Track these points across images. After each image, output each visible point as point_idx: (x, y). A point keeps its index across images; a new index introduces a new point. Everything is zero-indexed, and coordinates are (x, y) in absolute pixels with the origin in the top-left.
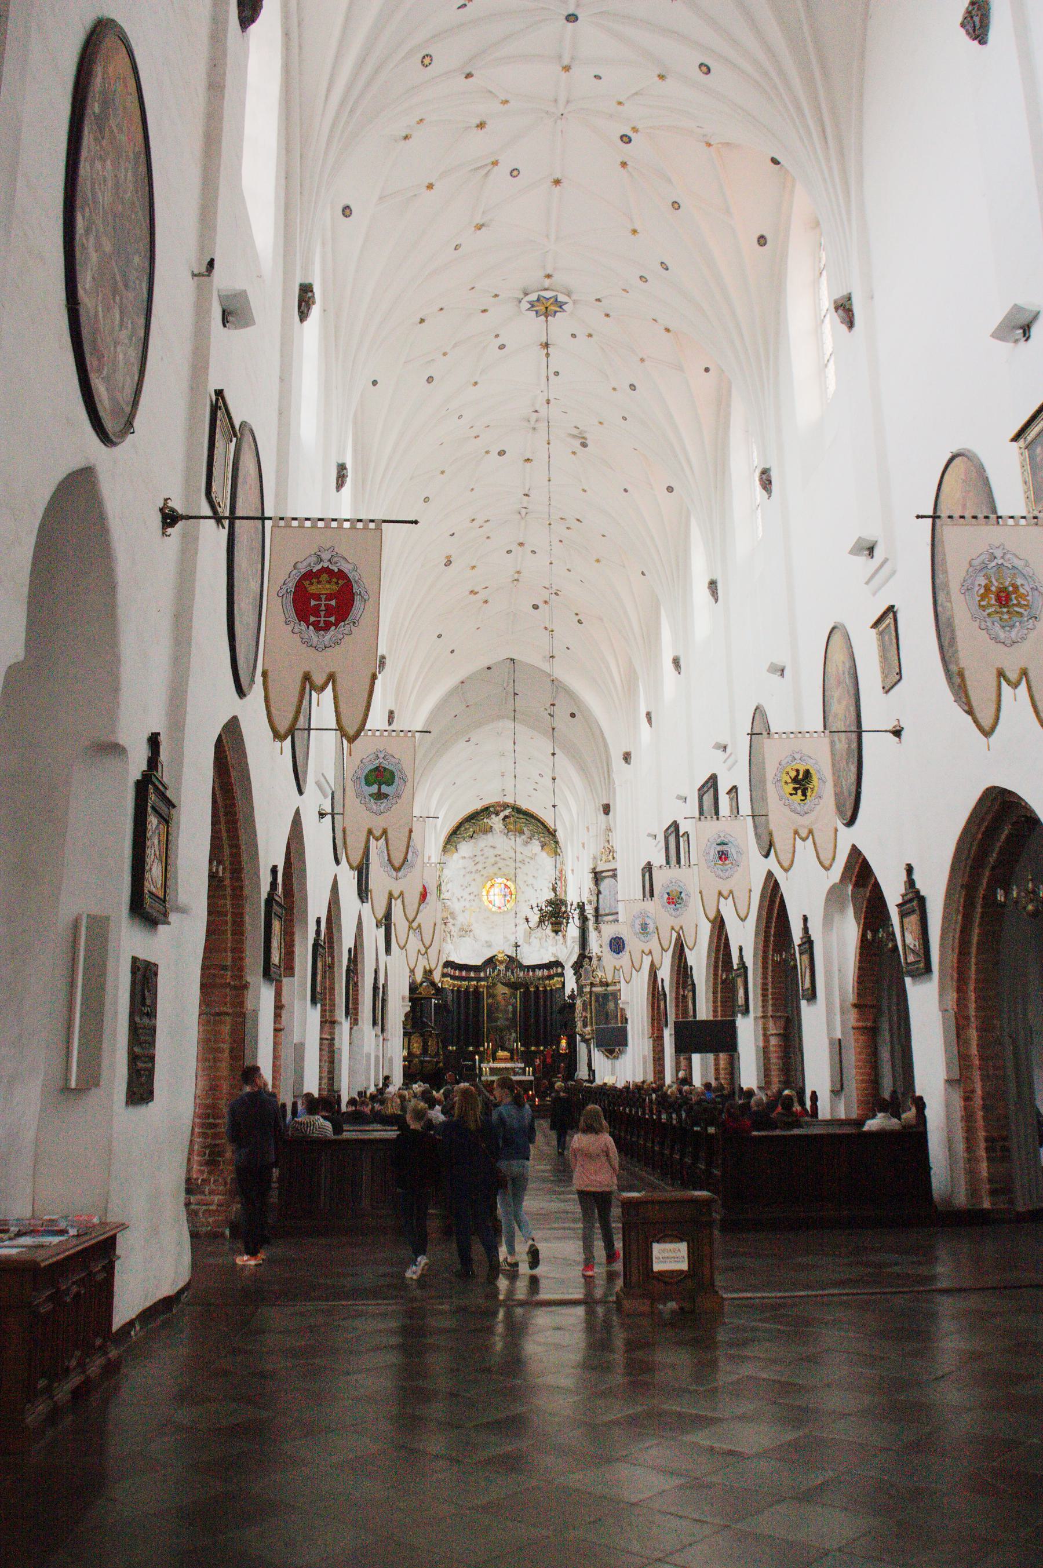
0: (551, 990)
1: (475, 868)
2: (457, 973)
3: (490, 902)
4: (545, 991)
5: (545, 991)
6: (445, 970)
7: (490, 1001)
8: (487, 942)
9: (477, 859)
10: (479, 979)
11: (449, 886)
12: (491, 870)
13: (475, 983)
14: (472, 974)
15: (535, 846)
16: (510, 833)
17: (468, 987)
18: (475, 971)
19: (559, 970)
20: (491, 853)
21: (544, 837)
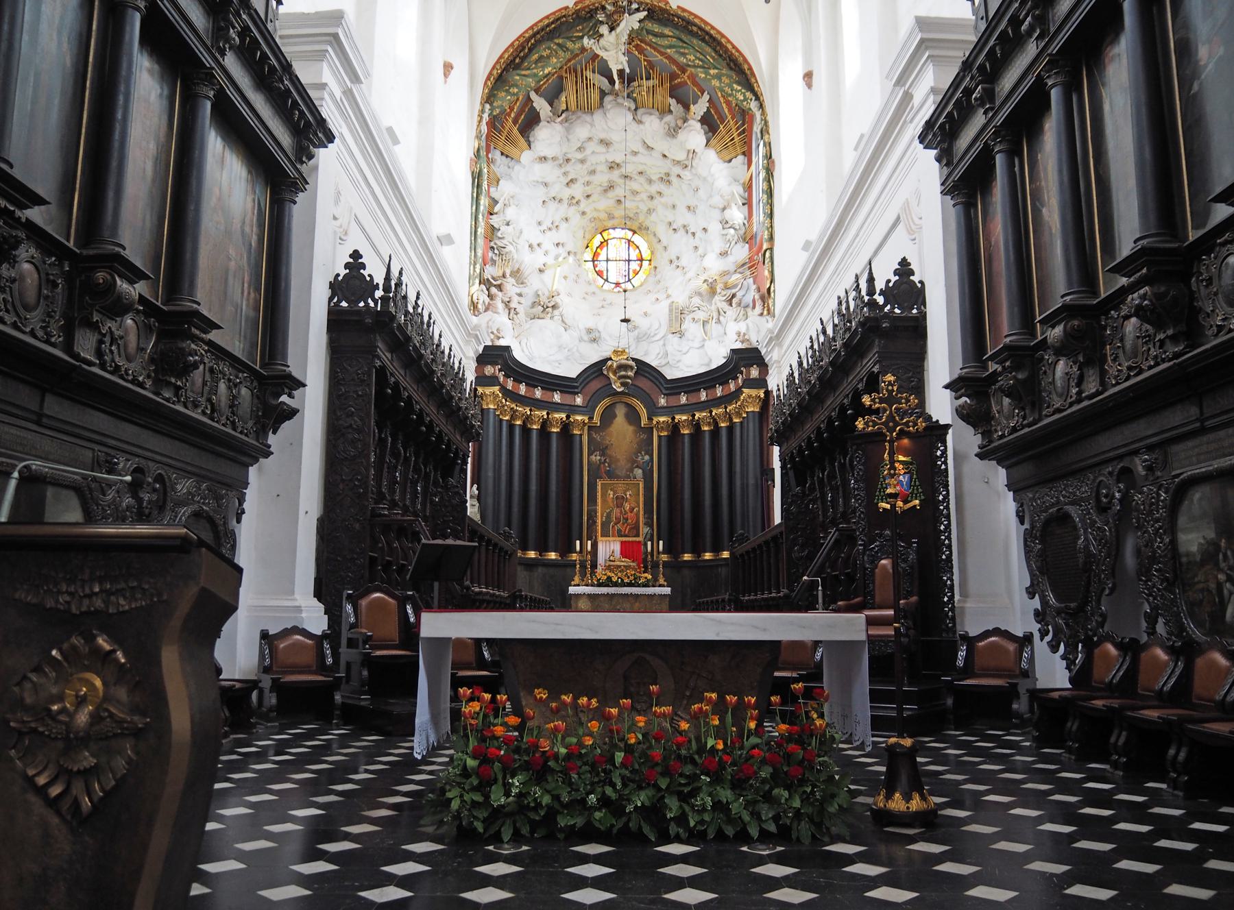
0: (731, 429)
1: (566, 193)
2: (523, 389)
3: (599, 273)
4: (716, 432)
5: (716, 432)
6: (489, 370)
7: (596, 458)
8: (589, 331)
9: (575, 170)
10: (572, 409)
11: (510, 213)
12: (604, 204)
13: (564, 416)
14: (557, 398)
15: (695, 136)
16: (640, 111)
17: (545, 424)
18: (561, 391)
19: (754, 373)
20: (600, 157)
21: (718, 77)
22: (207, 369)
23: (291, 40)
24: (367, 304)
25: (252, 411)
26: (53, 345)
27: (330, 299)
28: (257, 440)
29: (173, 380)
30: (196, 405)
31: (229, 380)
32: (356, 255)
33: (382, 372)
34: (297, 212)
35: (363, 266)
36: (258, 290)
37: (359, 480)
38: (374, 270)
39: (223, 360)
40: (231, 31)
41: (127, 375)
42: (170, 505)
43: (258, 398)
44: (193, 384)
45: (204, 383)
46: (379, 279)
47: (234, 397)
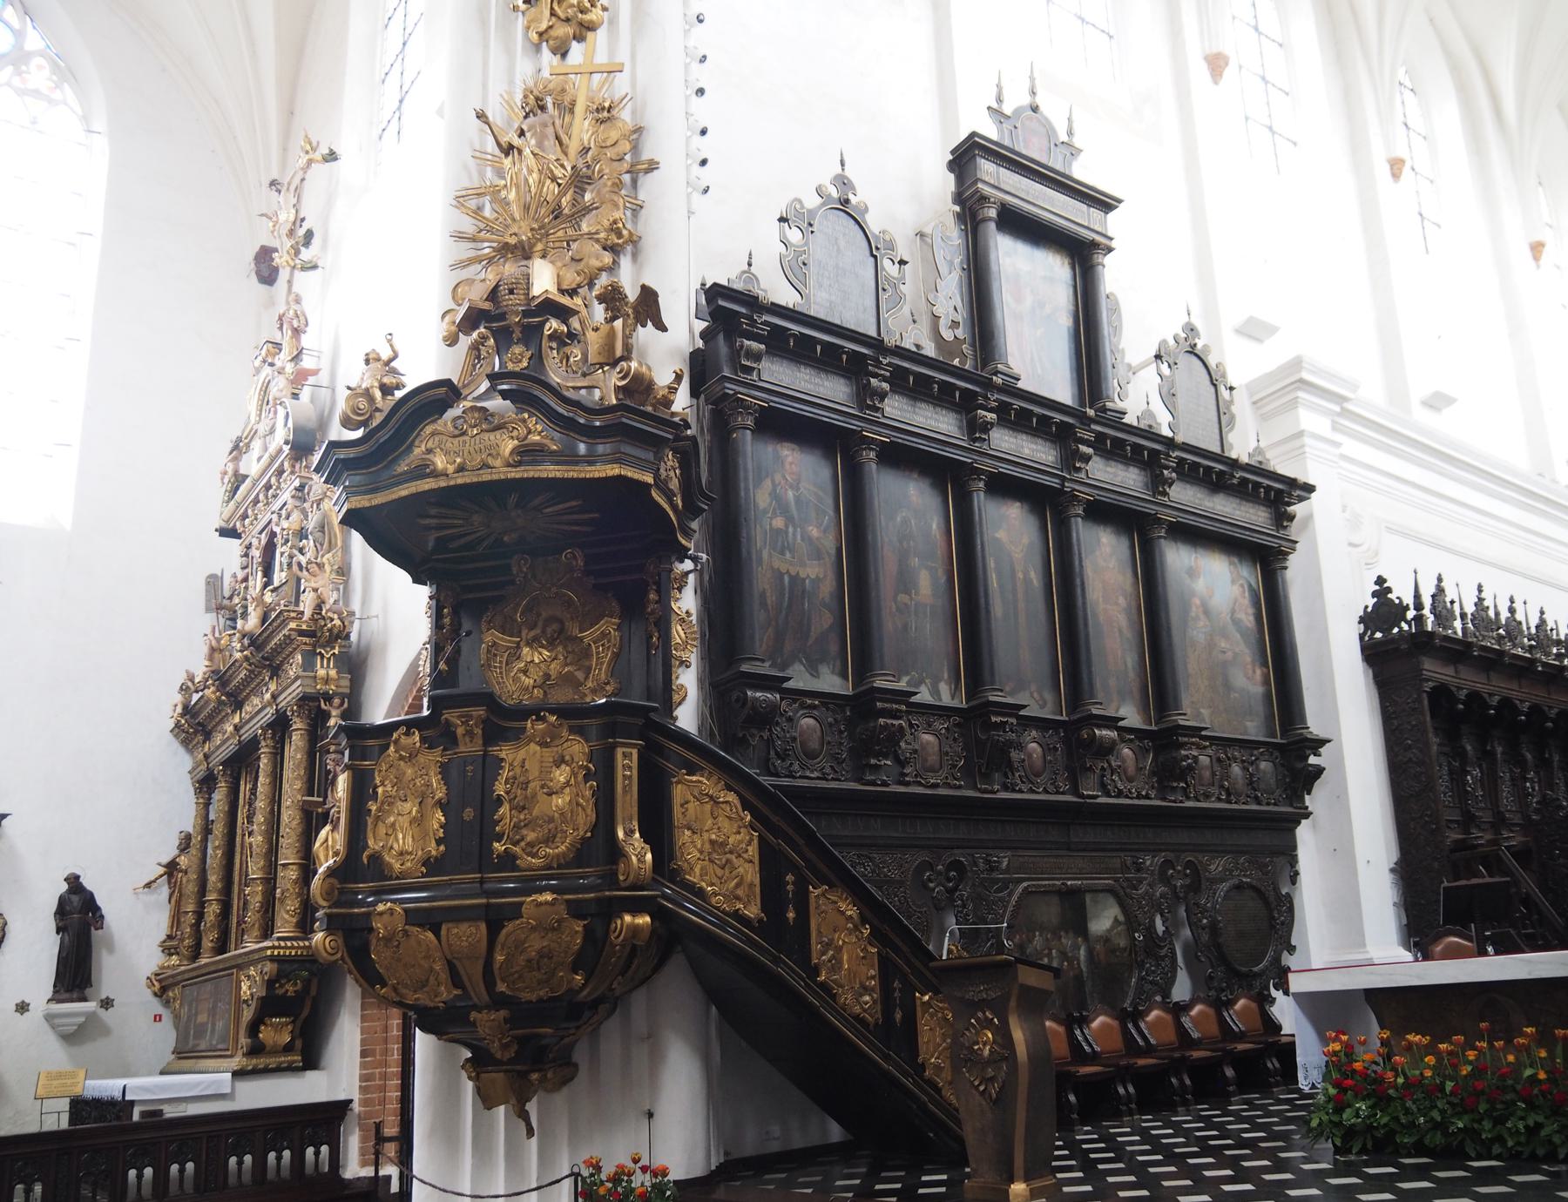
22: (1214, 760)
23: (1265, 401)
24: (1400, 628)
25: (1277, 780)
26: (1063, 793)
27: (1361, 637)
28: (1291, 805)
29: (1175, 784)
30: (1207, 796)
31: (1243, 761)
32: (1380, 581)
33: (1441, 694)
34: (1295, 572)
35: (1389, 590)
36: (1265, 664)
37: (1430, 816)
38: (1402, 592)
39: (1229, 746)
40: (1165, 472)
41: (1131, 793)
42: (1204, 884)
43: (1283, 765)
44: (1201, 778)
45: (1213, 774)
46: (1409, 600)
47: (1251, 775)
